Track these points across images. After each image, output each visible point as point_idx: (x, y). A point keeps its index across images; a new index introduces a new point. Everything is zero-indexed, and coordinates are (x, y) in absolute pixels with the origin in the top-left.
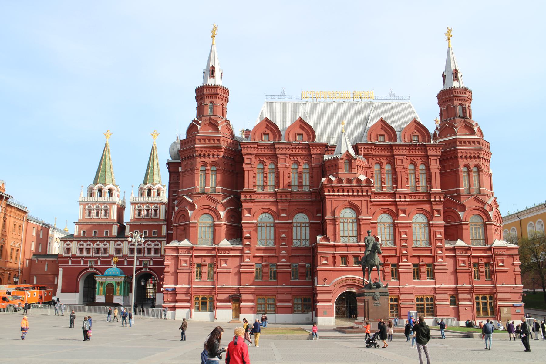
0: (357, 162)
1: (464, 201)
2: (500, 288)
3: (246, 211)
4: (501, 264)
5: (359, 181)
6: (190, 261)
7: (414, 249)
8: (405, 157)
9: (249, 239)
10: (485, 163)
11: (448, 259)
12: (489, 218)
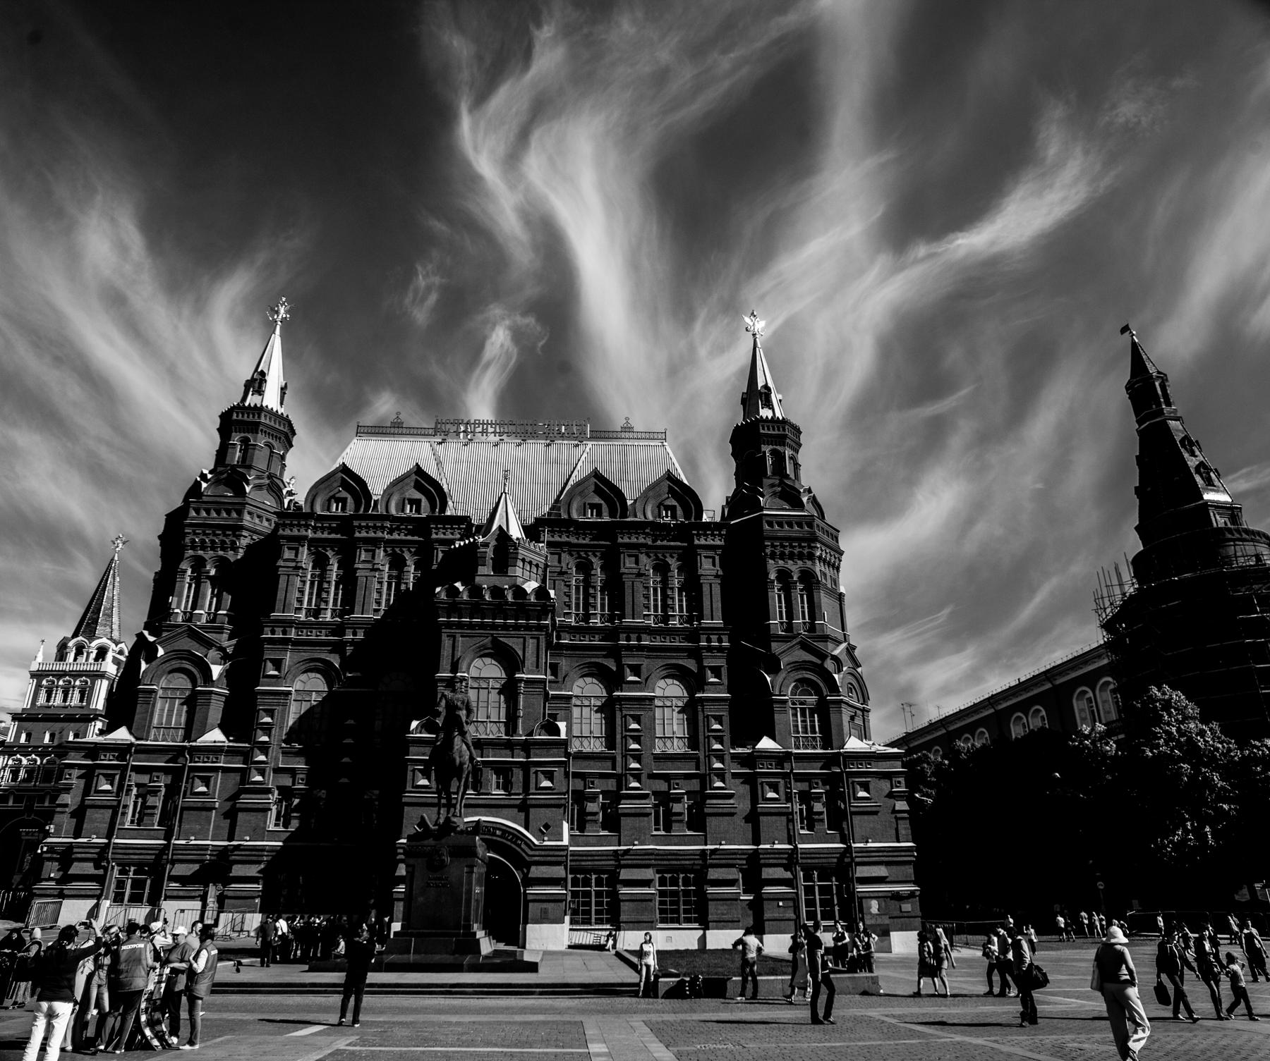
0: (521, 551)
1: (776, 647)
2: (861, 850)
3: (269, 665)
4: (862, 794)
5: (520, 592)
6: (122, 779)
7: (657, 758)
8: (644, 550)
9: (267, 729)
10: (829, 572)
11: (738, 781)
12: (834, 688)
